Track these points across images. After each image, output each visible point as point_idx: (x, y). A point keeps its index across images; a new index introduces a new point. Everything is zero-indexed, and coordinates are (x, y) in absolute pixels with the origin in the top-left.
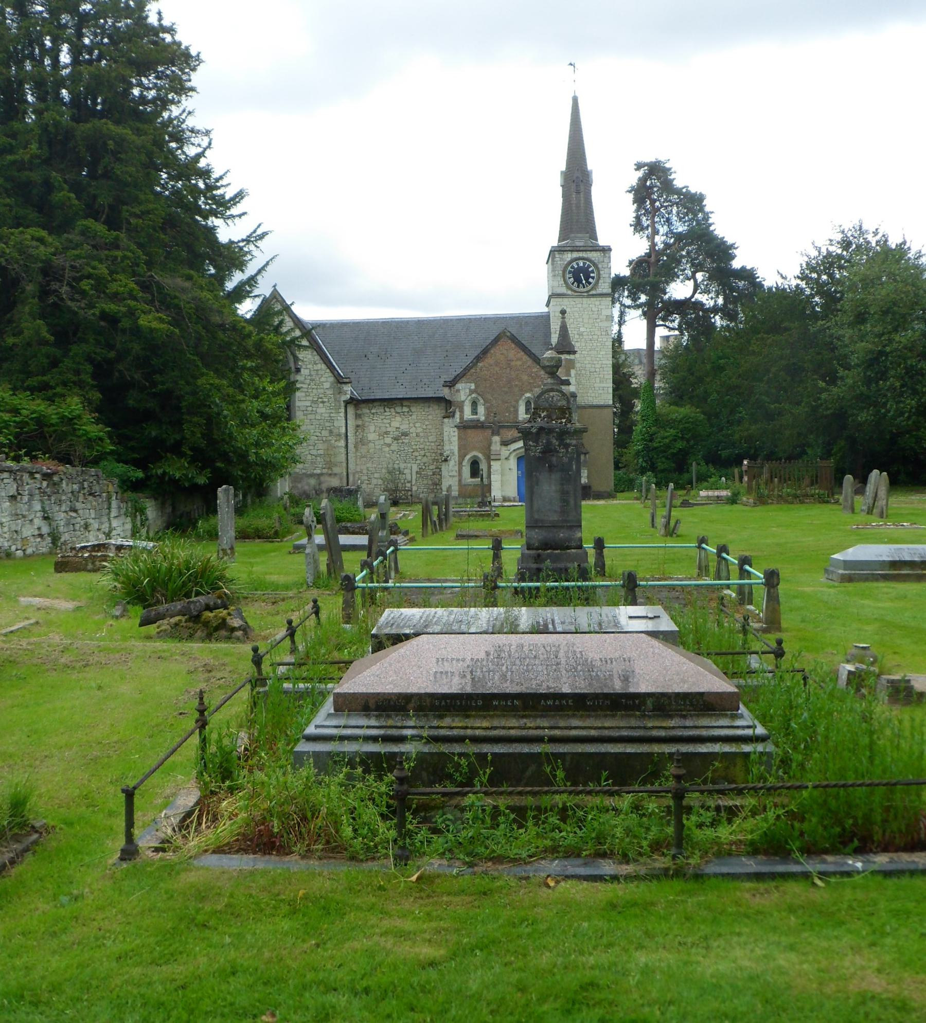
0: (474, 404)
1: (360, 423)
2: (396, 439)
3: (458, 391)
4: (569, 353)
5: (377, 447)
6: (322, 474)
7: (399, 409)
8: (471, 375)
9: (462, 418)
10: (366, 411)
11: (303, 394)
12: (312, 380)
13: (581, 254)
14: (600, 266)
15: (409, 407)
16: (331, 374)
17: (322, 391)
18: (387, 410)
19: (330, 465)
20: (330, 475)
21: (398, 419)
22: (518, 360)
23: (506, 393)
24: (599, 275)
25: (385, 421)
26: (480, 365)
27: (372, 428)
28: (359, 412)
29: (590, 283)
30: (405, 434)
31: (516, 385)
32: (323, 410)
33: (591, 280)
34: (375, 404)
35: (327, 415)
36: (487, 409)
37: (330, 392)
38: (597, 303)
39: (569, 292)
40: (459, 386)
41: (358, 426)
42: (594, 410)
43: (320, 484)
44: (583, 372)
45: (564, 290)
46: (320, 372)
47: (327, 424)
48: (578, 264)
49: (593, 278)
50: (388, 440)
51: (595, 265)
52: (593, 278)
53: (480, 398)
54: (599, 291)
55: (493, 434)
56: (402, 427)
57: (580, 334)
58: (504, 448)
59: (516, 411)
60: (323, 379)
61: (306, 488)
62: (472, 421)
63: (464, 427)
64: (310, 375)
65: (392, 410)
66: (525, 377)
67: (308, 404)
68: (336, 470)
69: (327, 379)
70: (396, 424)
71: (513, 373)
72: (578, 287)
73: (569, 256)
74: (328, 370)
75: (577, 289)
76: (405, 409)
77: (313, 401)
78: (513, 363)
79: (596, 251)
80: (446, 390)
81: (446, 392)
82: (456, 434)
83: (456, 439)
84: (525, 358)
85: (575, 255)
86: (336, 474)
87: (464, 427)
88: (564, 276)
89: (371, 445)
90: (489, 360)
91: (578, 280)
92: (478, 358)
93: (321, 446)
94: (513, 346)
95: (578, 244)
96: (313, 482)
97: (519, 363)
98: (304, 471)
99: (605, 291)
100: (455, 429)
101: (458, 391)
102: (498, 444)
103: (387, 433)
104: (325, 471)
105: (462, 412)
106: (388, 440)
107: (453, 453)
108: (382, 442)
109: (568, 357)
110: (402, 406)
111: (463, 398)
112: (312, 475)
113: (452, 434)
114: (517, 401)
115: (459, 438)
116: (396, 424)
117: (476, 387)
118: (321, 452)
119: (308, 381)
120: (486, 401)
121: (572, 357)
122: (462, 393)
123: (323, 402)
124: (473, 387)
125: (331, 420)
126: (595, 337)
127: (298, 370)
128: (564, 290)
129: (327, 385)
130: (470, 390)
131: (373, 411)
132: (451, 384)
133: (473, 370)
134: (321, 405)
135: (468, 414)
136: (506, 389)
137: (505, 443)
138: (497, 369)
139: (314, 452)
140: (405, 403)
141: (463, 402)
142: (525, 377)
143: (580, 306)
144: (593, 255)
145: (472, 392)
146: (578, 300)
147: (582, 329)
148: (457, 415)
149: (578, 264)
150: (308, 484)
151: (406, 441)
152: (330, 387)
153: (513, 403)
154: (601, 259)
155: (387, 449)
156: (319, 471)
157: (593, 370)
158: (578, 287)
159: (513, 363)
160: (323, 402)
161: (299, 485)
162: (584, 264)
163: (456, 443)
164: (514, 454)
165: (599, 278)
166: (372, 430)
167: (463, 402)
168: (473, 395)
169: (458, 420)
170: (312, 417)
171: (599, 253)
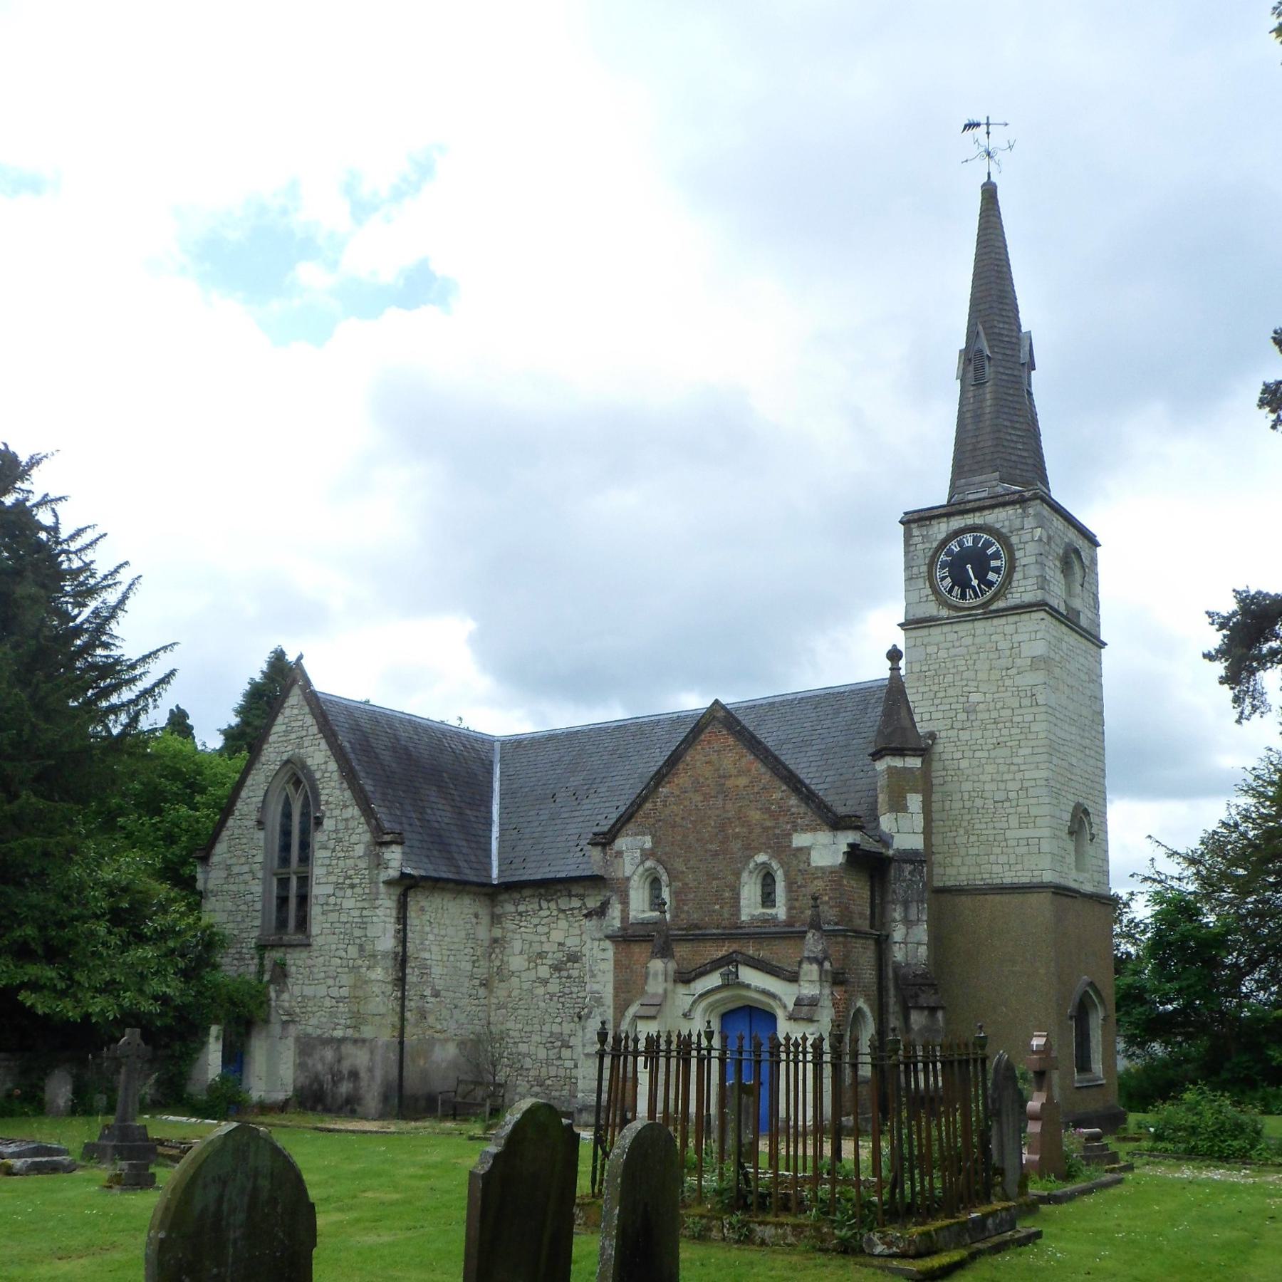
0: (655, 883)
1: (497, 933)
2: (557, 968)
3: (619, 854)
4: (900, 752)
5: (525, 986)
6: (342, 1040)
7: (564, 903)
8: (647, 816)
9: (625, 918)
10: (510, 908)
11: (323, 871)
12: (339, 841)
13: (969, 520)
14: (1014, 540)
15: (581, 897)
16: (366, 827)
17: (350, 862)
18: (544, 905)
19: (358, 1019)
20: (355, 1041)
21: (563, 924)
22: (740, 773)
23: (716, 854)
24: (1012, 561)
25: (541, 929)
26: (663, 790)
27: (517, 945)
28: (498, 910)
29: (990, 584)
30: (574, 958)
31: (737, 836)
32: (349, 903)
33: (992, 576)
34: (527, 892)
35: (357, 913)
36: (675, 894)
37: (362, 865)
38: (1010, 629)
39: (944, 612)
40: (622, 843)
41: (495, 941)
42: (1006, 898)
43: (339, 1061)
44: (979, 802)
45: (932, 609)
46: (352, 824)
47: (357, 933)
48: (961, 544)
49: (997, 570)
50: (544, 971)
51: (1003, 539)
52: (997, 570)
53: (661, 869)
54: (1014, 598)
55: (654, 955)
56: (569, 942)
57: (970, 710)
58: (681, 989)
59: (736, 898)
60: (355, 838)
61: (319, 1067)
62: (643, 924)
63: (627, 938)
64: (336, 831)
65: (553, 905)
66: (755, 816)
67: (329, 889)
68: (367, 1032)
69: (361, 836)
70: (557, 936)
71: (729, 805)
72: (963, 596)
73: (941, 529)
74: (362, 820)
75: (960, 603)
76: (576, 903)
77: (338, 885)
78: (729, 783)
79: (1004, 505)
80: (596, 853)
81: (594, 861)
82: (610, 954)
83: (609, 966)
84: (758, 768)
85: (957, 523)
86: (364, 1041)
87: (627, 937)
88: (931, 577)
89: (515, 980)
90: (682, 779)
91: (964, 584)
92: (660, 778)
93: (346, 979)
94: (731, 741)
95: (971, 497)
96: (329, 1054)
97: (742, 781)
98: (319, 1032)
99: (1028, 598)
100: (608, 944)
101: (619, 854)
102: (661, 978)
103: (541, 955)
104: (350, 1032)
105: (625, 902)
106: (544, 971)
107: (599, 1001)
108: (532, 975)
109: (898, 762)
110: (570, 896)
111: (628, 870)
112: (331, 1040)
113: (601, 955)
114: (738, 875)
115: (617, 964)
116: (557, 936)
117: (656, 842)
118: (344, 992)
119: (332, 844)
120: (673, 877)
121: (914, 762)
122: (627, 858)
123: (352, 886)
124: (648, 845)
125: (363, 925)
126: (1008, 712)
127: (319, 822)
128: (932, 609)
129: (360, 850)
130: (642, 850)
131: (521, 908)
132: (605, 840)
133: (648, 805)
134: (349, 892)
135: (639, 906)
136: (714, 847)
137: (685, 977)
138: (697, 798)
139: (335, 992)
140: (576, 889)
141: (628, 879)
142: (755, 816)
143: (968, 640)
144: (999, 518)
145: (646, 855)
146: (964, 628)
147: (974, 698)
148: (615, 911)
149: (961, 544)
150: (322, 1059)
151: (575, 973)
152: (365, 854)
153: (731, 878)
154: (1017, 523)
155: (540, 991)
156: (339, 1033)
157: (1000, 796)
158: (963, 596)
159: (729, 783)
160: (352, 886)
161: (310, 1062)
162: (976, 540)
163: (610, 977)
164: (703, 1004)
165: (1012, 568)
166: (517, 951)
167: (628, 879)
168: (648, 864)
169: (617, 923)
170: (333, 917)
171: (1010, 511)
